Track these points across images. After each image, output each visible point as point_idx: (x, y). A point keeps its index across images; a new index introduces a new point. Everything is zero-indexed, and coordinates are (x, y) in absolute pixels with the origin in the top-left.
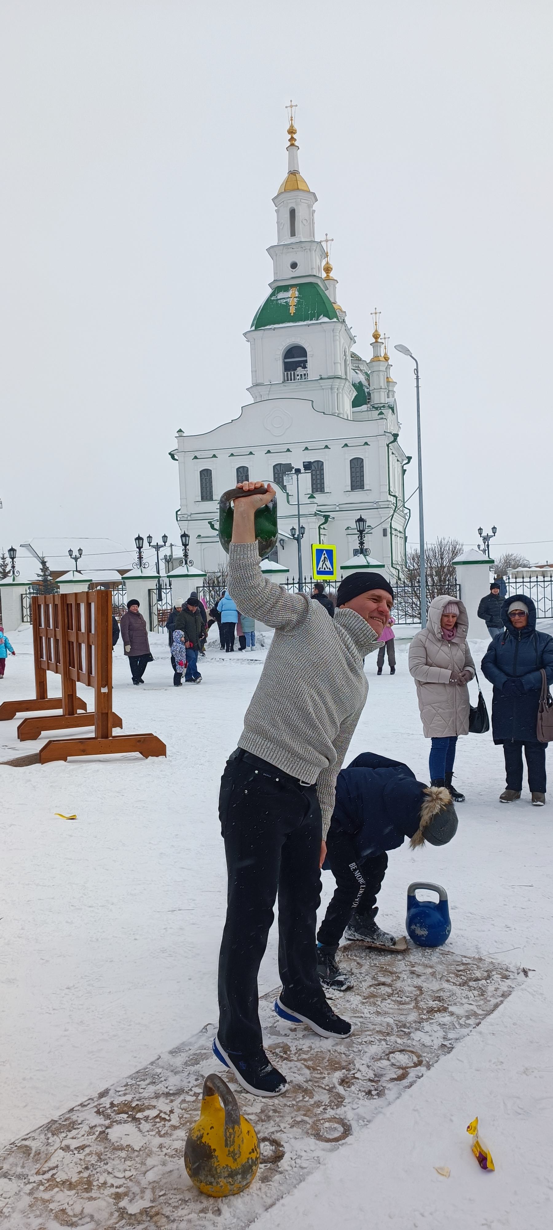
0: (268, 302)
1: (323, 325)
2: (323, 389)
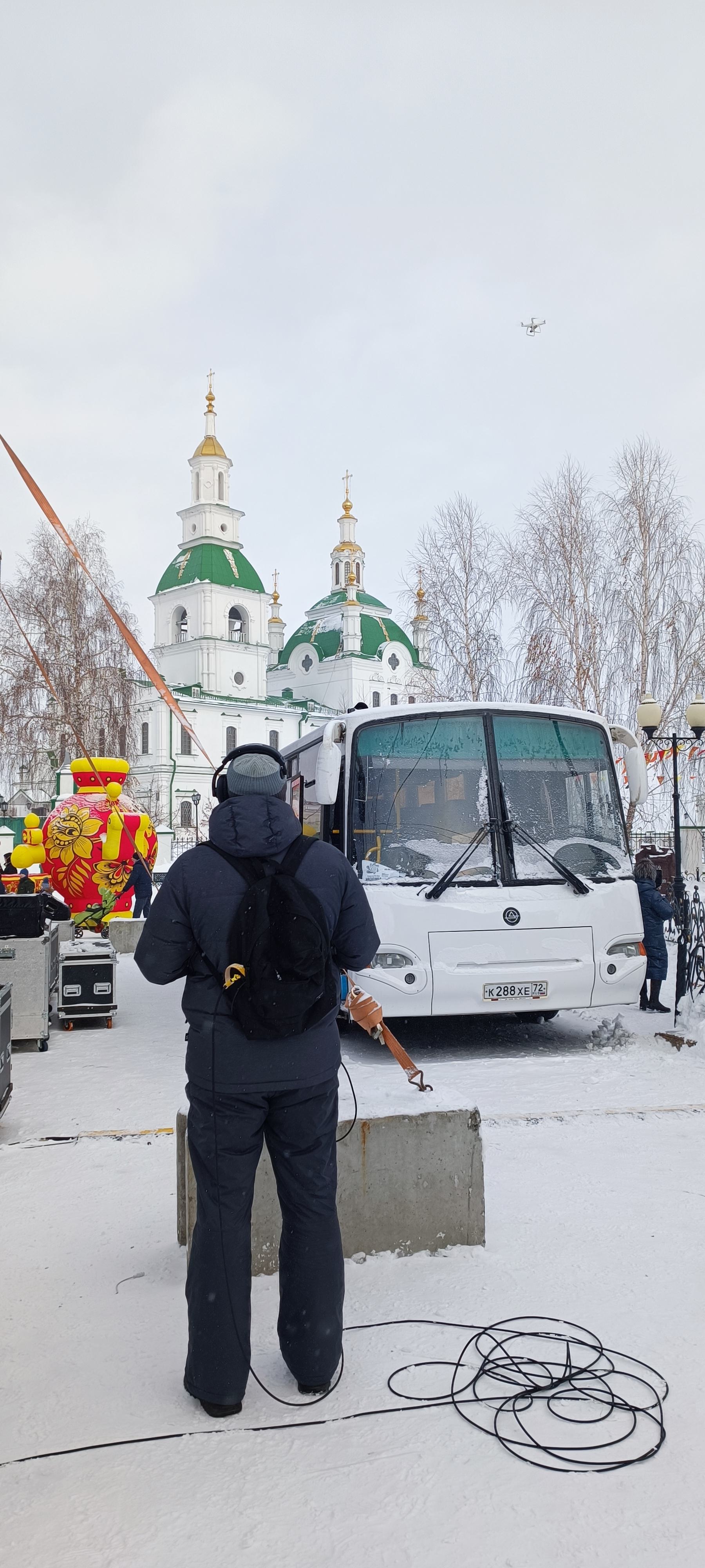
0: (171, 565)
1: (194, 587)
2: (195, 650)
